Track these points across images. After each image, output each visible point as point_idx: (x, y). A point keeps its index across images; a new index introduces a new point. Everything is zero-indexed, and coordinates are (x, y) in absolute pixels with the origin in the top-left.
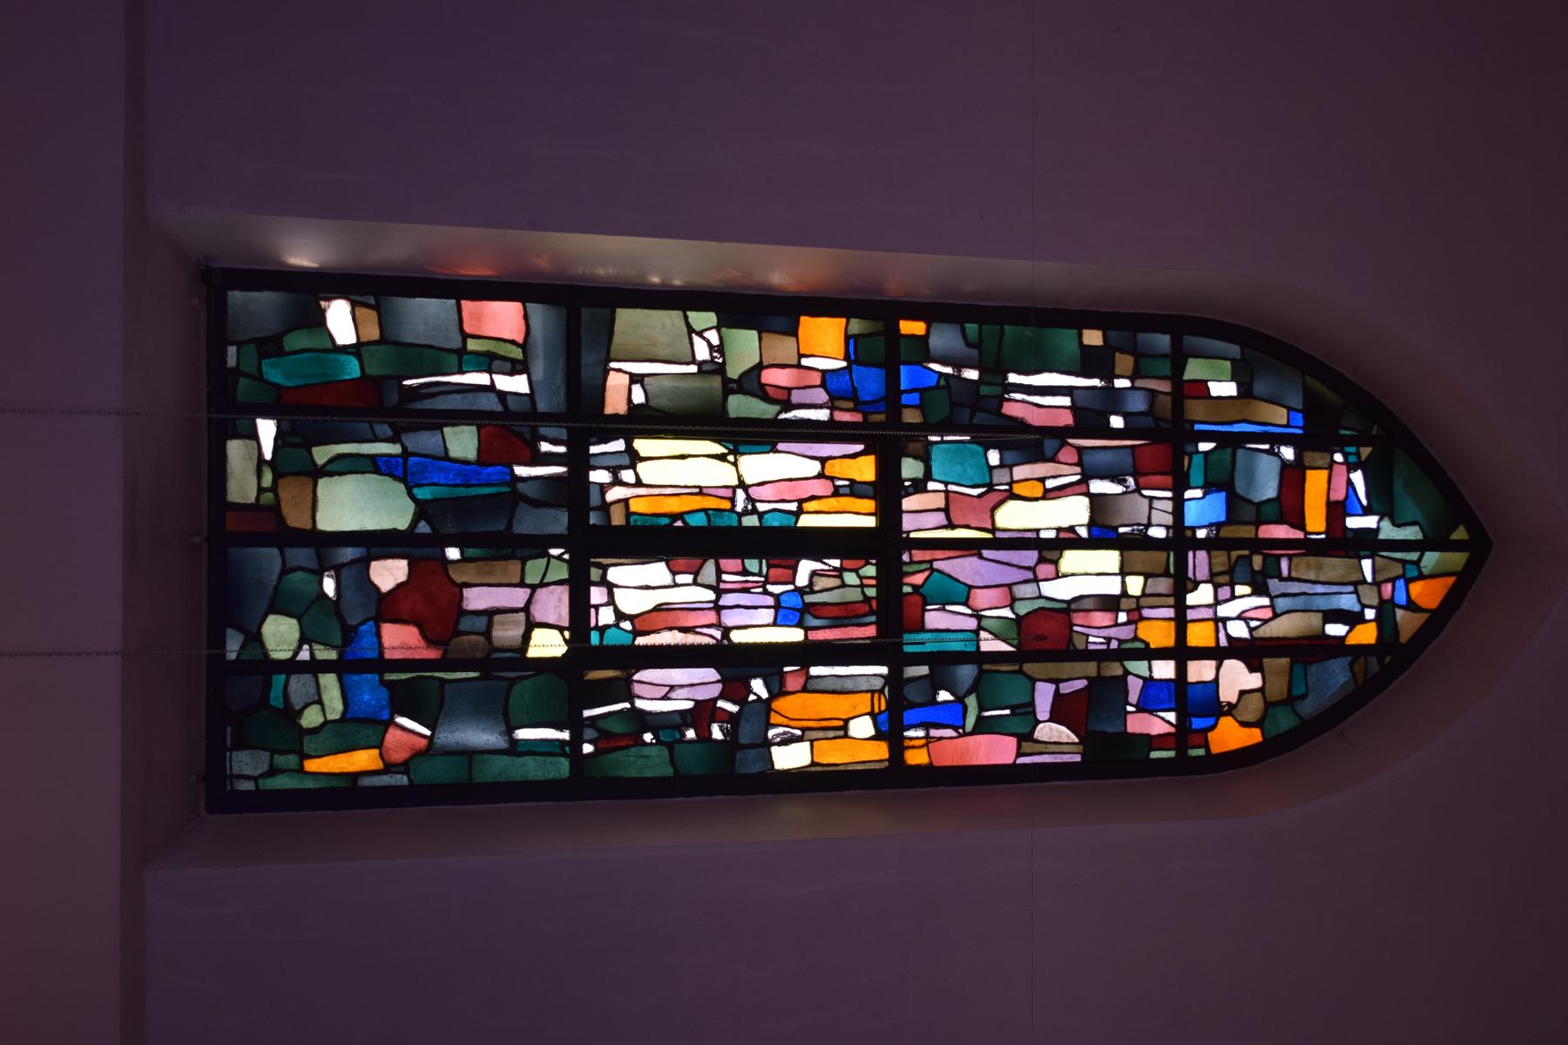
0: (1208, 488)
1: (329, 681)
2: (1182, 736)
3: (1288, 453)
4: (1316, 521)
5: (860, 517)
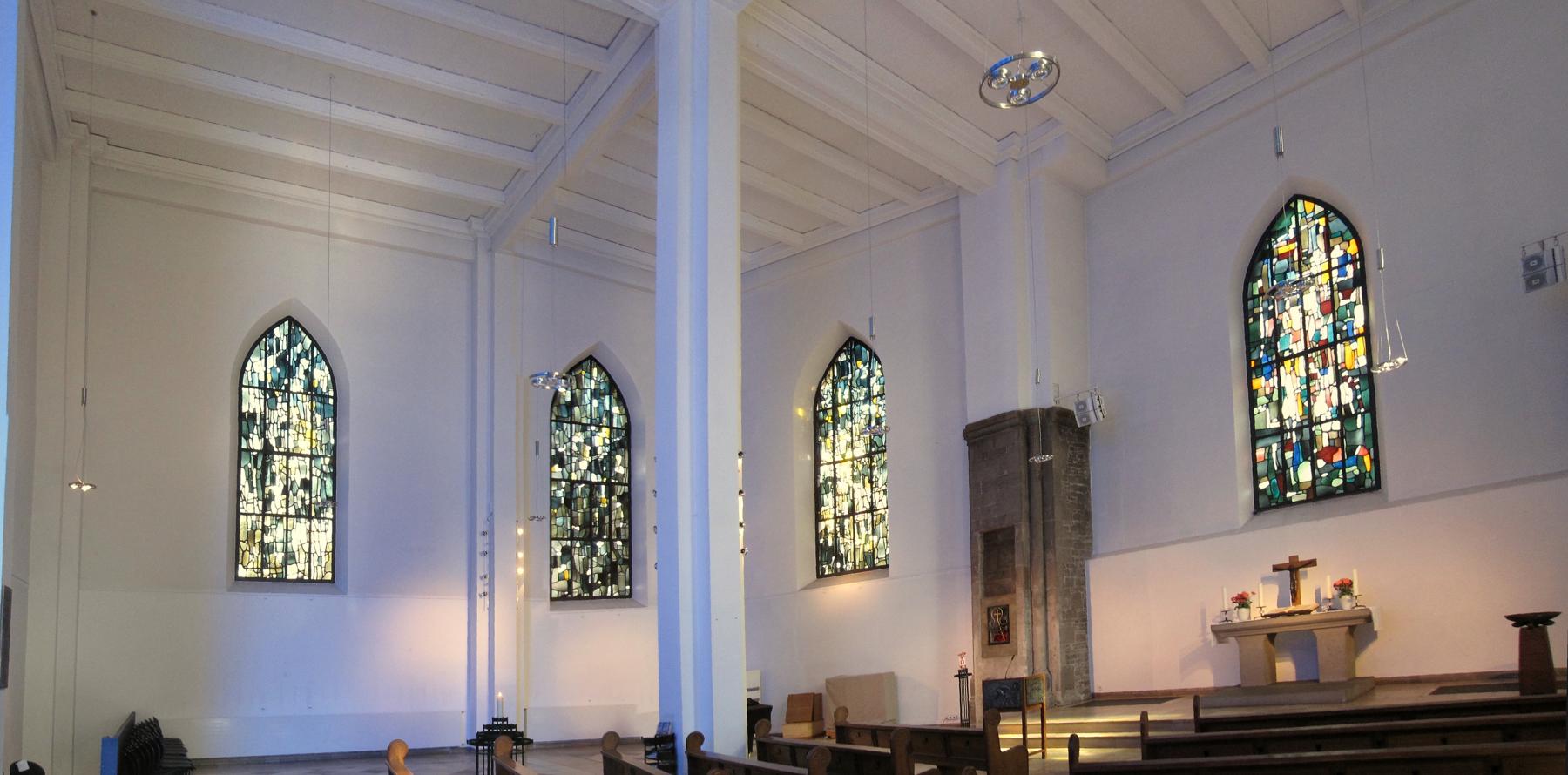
2: (1353, 262)
5: (1301, 361)
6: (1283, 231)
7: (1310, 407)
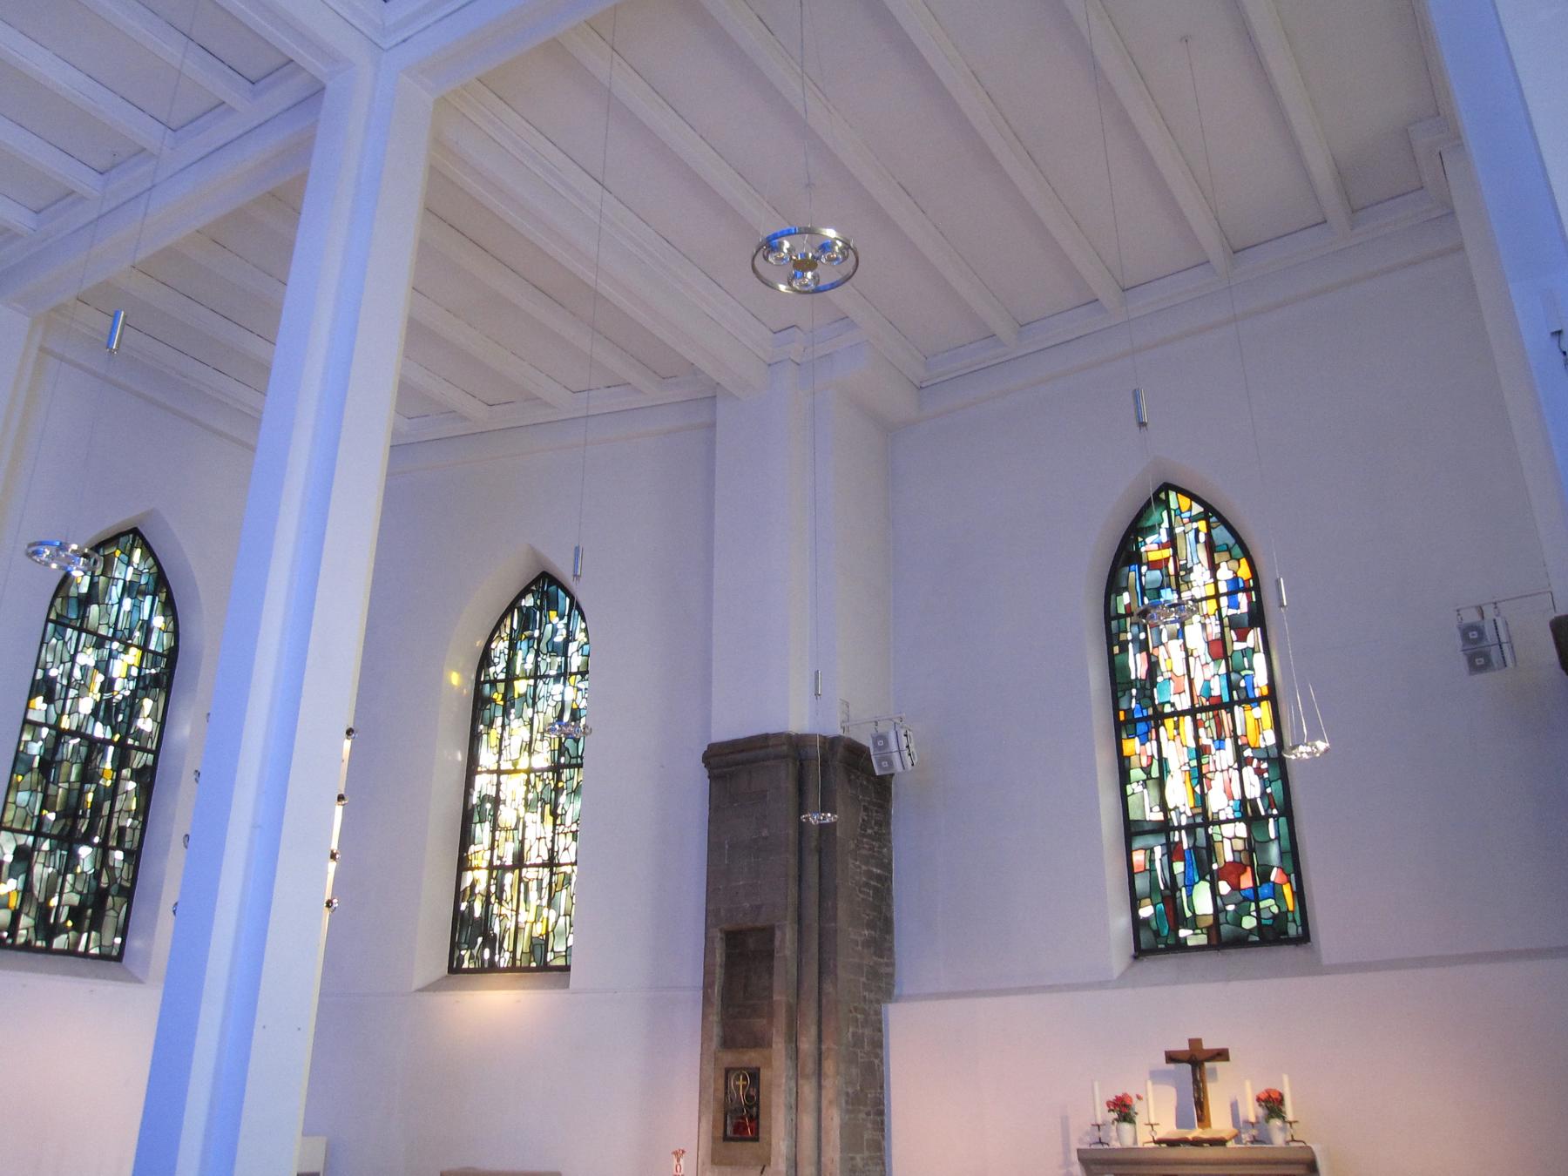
0: (1159, 596)
1: (1263, 904)
2: (1246, 590)
3: (1144, 569)
4: (1168, 552)
5: (1187, 722)
6: (1152, 530)
7: (1203, 796)
